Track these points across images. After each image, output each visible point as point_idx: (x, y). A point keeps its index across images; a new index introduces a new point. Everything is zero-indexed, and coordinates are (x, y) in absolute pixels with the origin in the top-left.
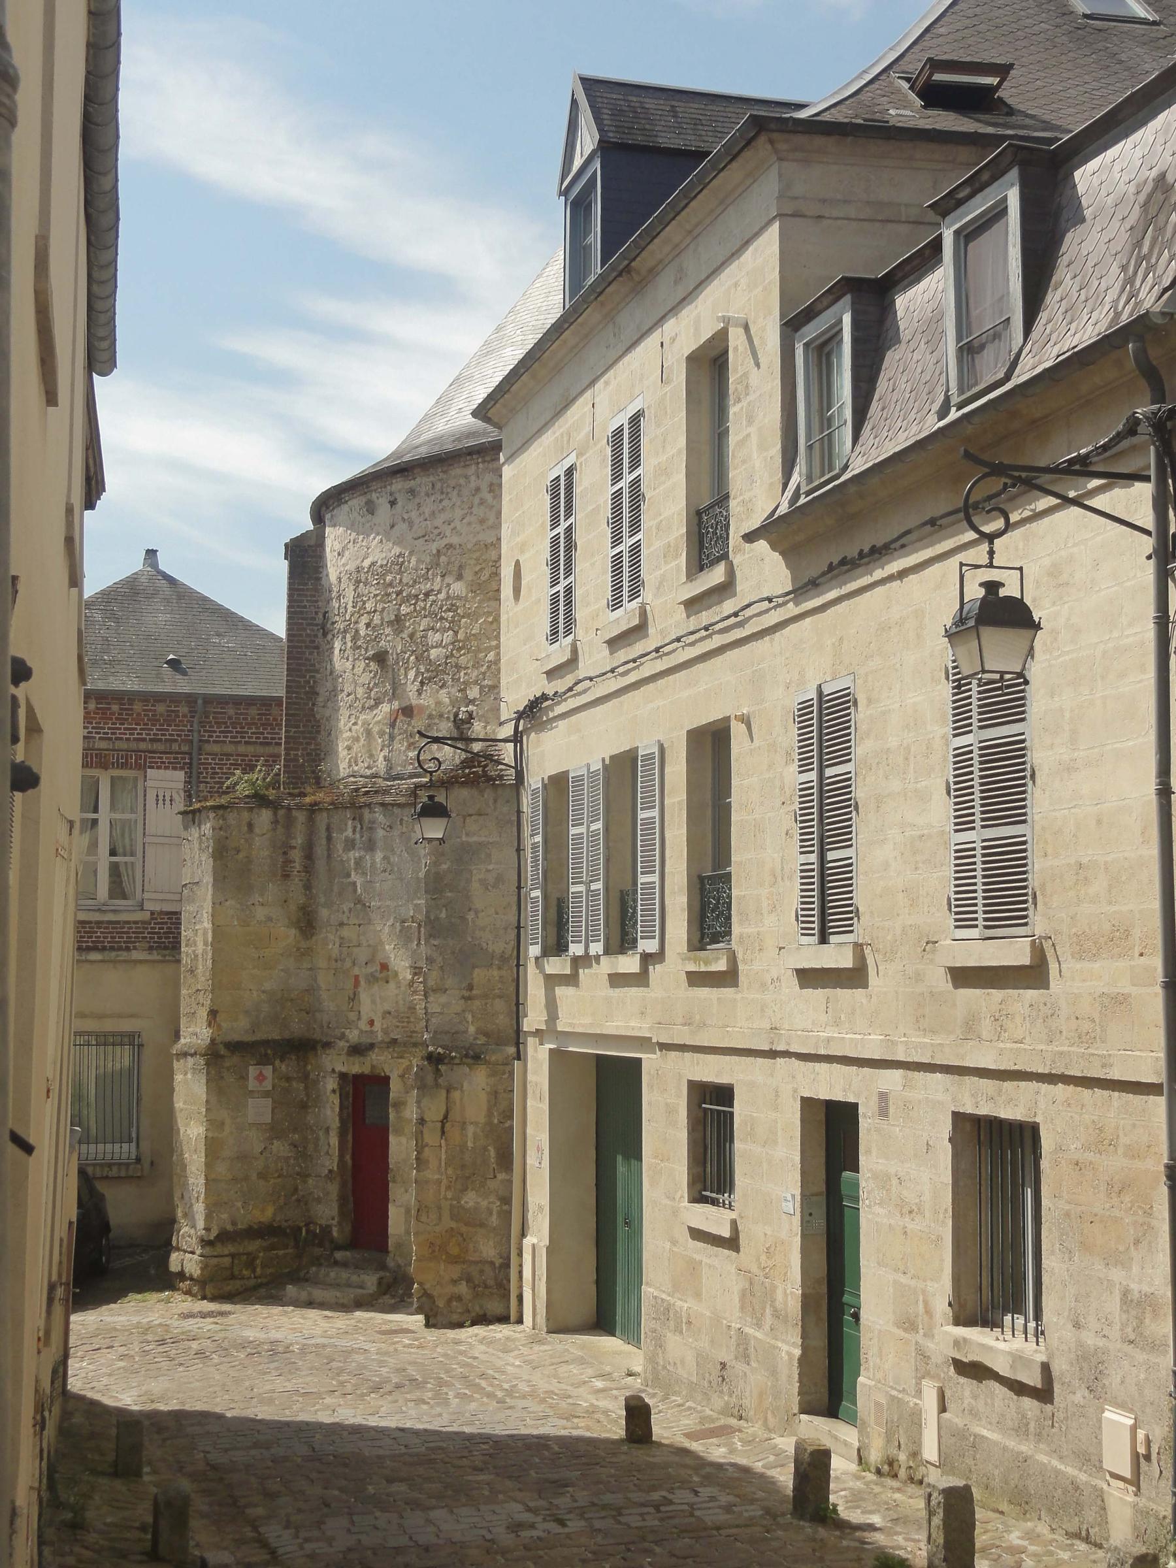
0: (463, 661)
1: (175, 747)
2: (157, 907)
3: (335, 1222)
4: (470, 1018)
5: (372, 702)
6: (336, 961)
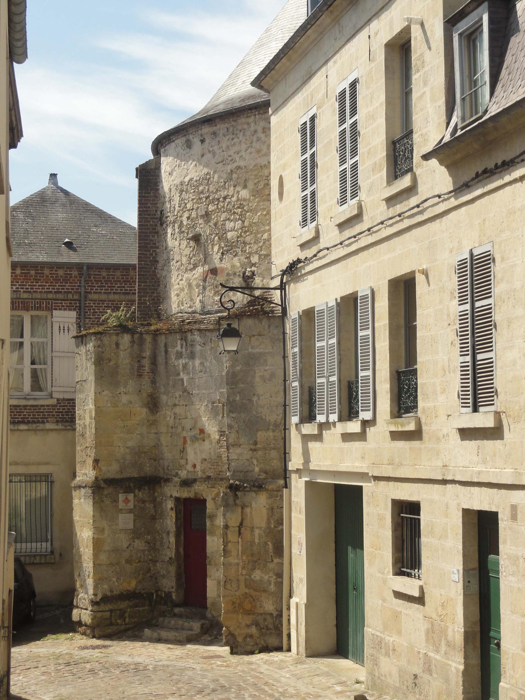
0: (248, 239)
1: (70, 296)
2: (61, 396)
3: (173, 590)
4: (255, 462)
5: (192, 266)
6: (172, 428)
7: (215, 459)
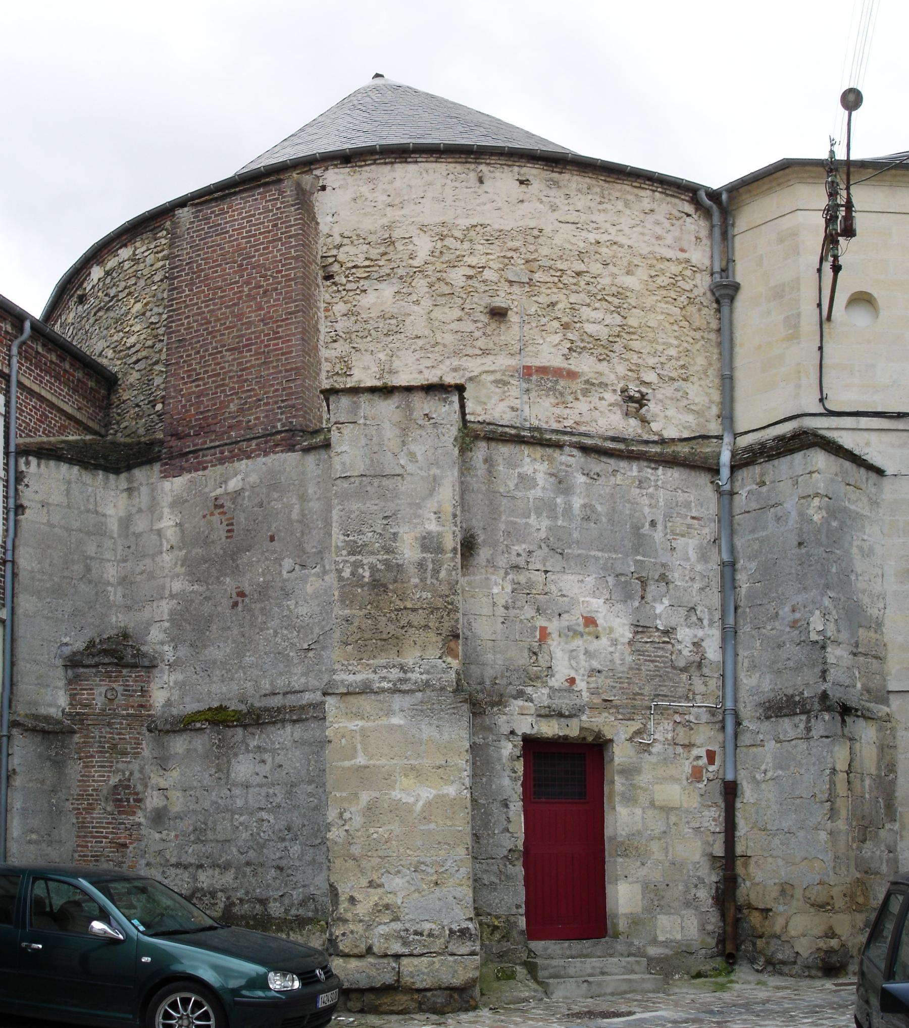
6: (507, 608)
7: (623, 672)
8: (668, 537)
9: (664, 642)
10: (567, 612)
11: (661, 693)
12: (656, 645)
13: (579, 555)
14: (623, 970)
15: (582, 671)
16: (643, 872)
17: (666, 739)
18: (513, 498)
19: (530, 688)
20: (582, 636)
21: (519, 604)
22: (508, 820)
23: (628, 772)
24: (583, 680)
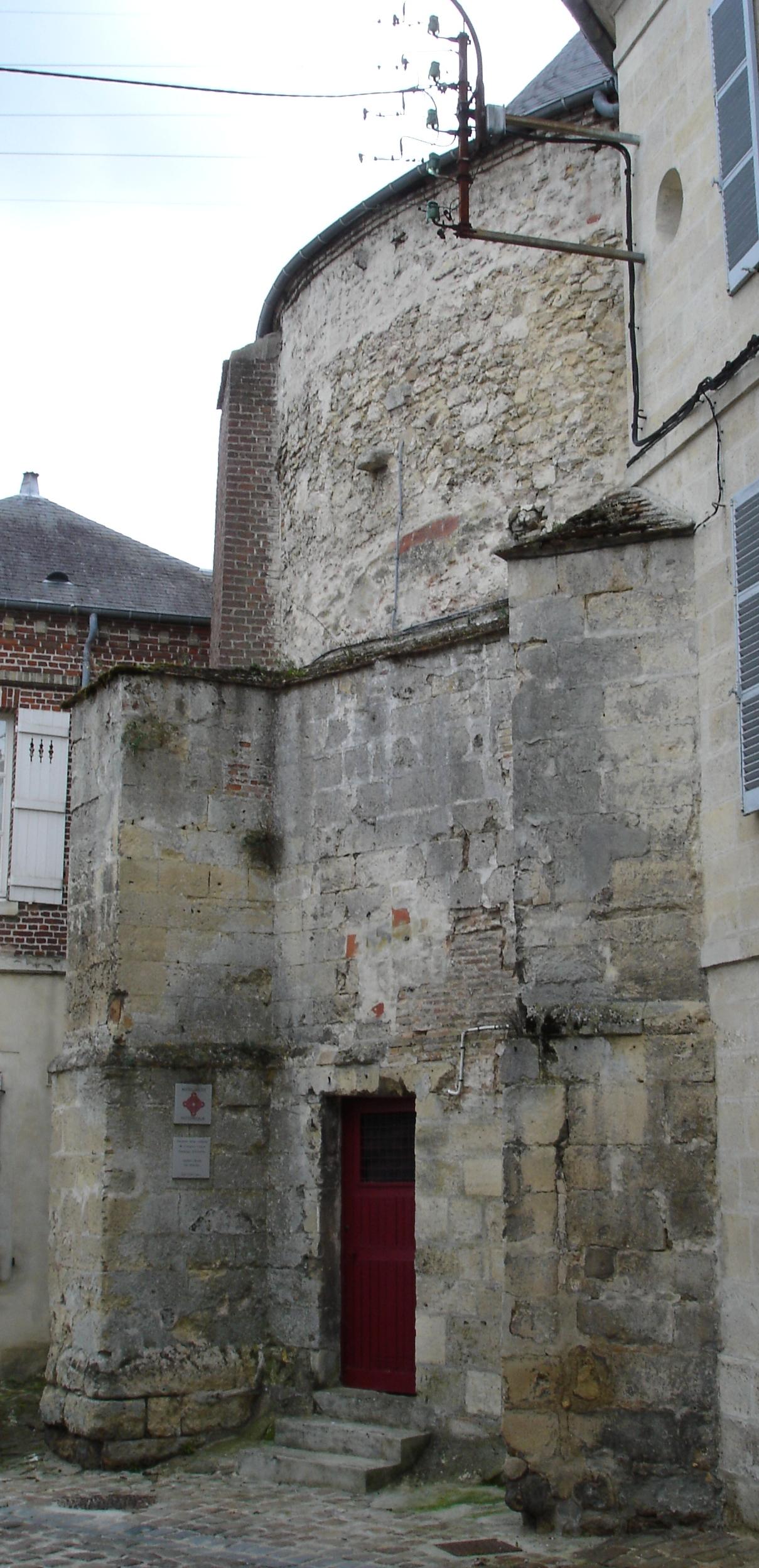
0: (524, 434)
1: (58, 680)
2: (29, 897)
3: (314, 1344)
4: (607, 953)
5: (365, 536)
6: (315, 917)
7: (439, 986)
8: (499, 755)
9: (494, 928)
10: (377, 908)
11: (487, 1011)
12: (482, 935)
13: (392, 821)
14: (370, 1450)
15: (391, 993)
16: (448, 1299)
17: (483, 1085)
18: (325, 759)
19: (337, 1026)
20: (390, 940)
21: (328, 908)
22: (304, 1215)
23: (437, 1139)
24: (392, 1006)
